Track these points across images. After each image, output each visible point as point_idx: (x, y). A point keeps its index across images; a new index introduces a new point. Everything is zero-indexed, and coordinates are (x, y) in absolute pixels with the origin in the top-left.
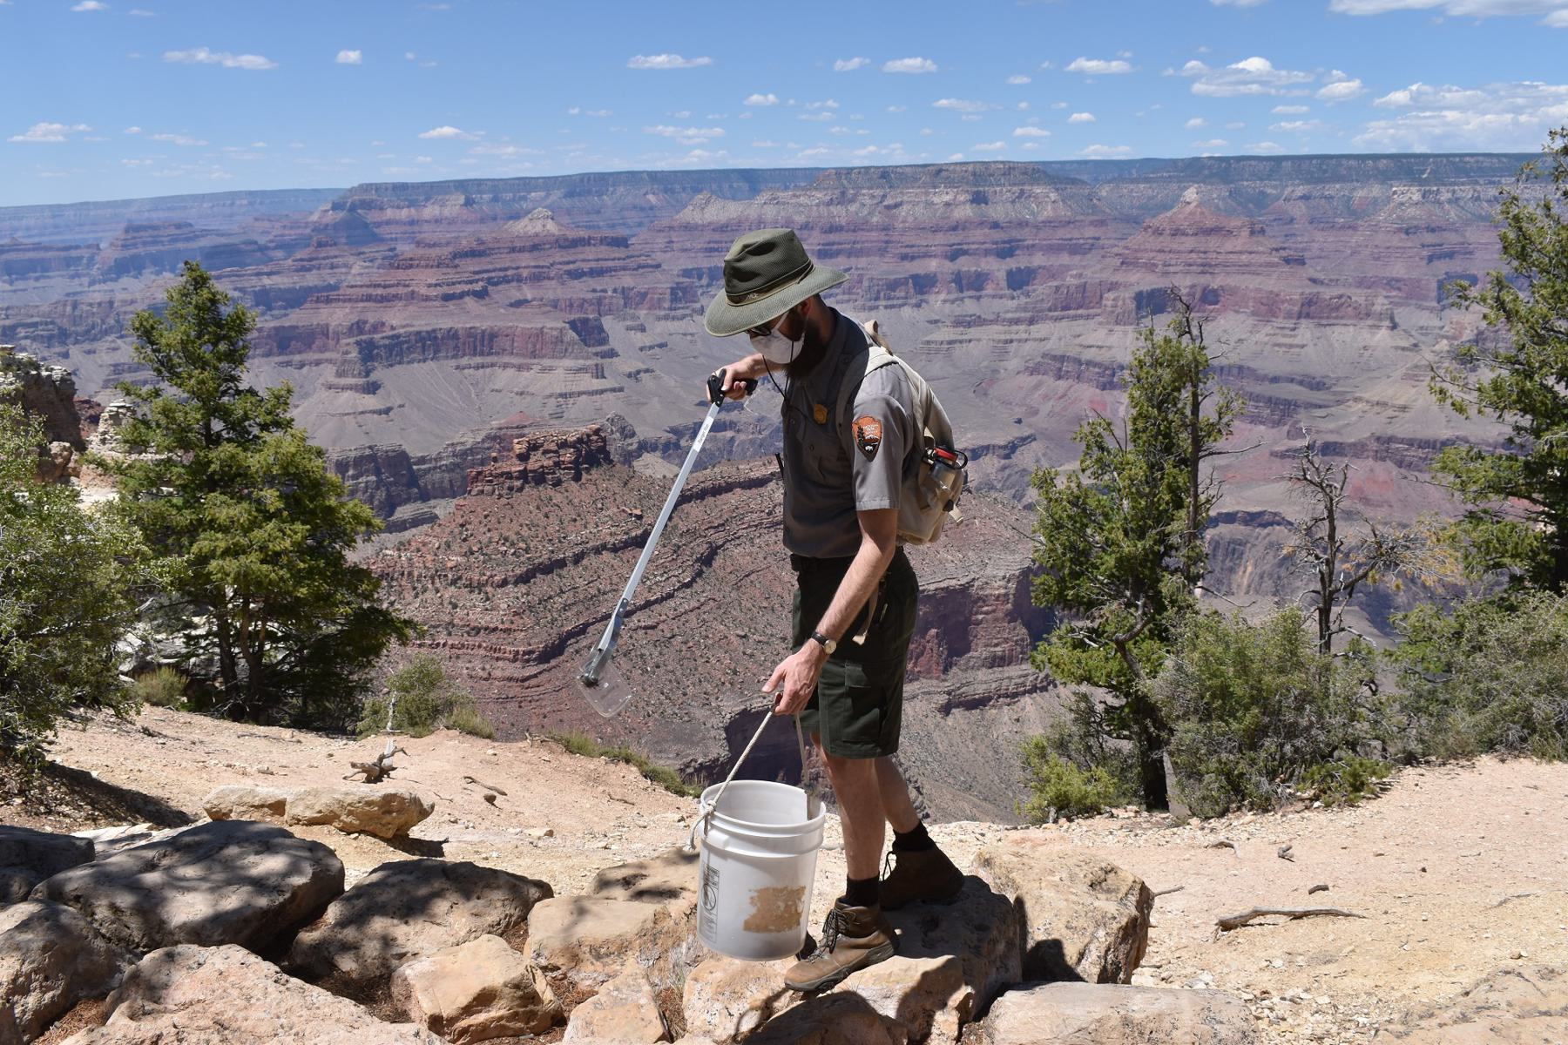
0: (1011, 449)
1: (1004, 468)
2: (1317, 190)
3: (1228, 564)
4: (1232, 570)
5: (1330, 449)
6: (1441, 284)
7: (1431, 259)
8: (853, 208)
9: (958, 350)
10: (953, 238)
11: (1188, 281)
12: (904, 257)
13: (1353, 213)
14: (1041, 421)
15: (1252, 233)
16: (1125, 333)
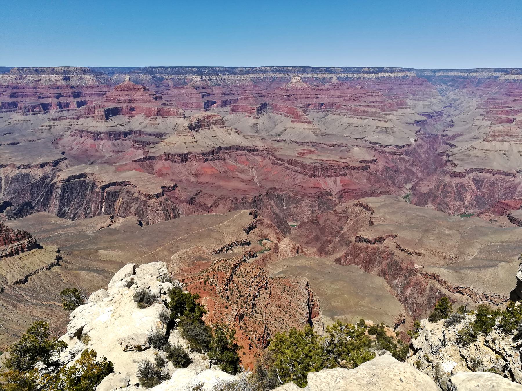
0: (56, 163)
1: (53, 170)
2: (175, 77)
3: (113, 199)
4: (115, 201)
5: (152, 158)
6: (205, 104)
7: (203, 97)
8: (25, 81)
9: (53, 129)
10: (57, 91)
11: (125, 105)
12: (39, 98)
13: (186, 83)
14: (73, 152)
15: (145, 90)
16: (102, 122)
